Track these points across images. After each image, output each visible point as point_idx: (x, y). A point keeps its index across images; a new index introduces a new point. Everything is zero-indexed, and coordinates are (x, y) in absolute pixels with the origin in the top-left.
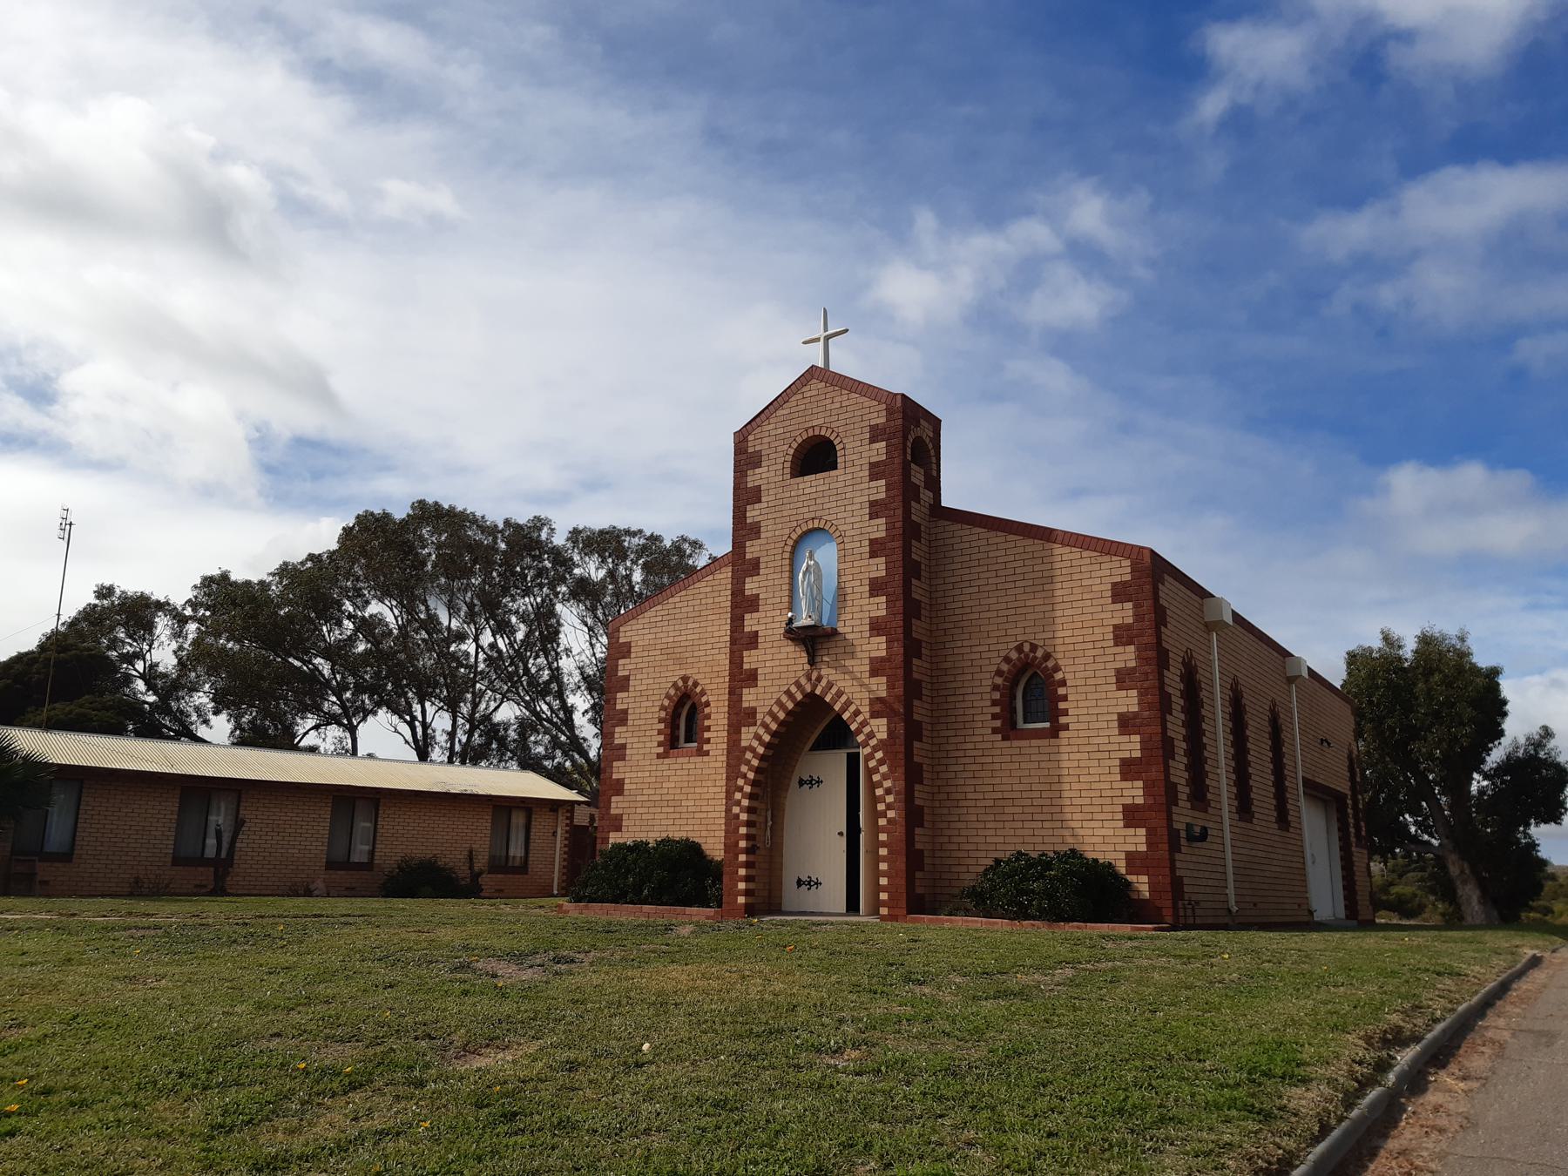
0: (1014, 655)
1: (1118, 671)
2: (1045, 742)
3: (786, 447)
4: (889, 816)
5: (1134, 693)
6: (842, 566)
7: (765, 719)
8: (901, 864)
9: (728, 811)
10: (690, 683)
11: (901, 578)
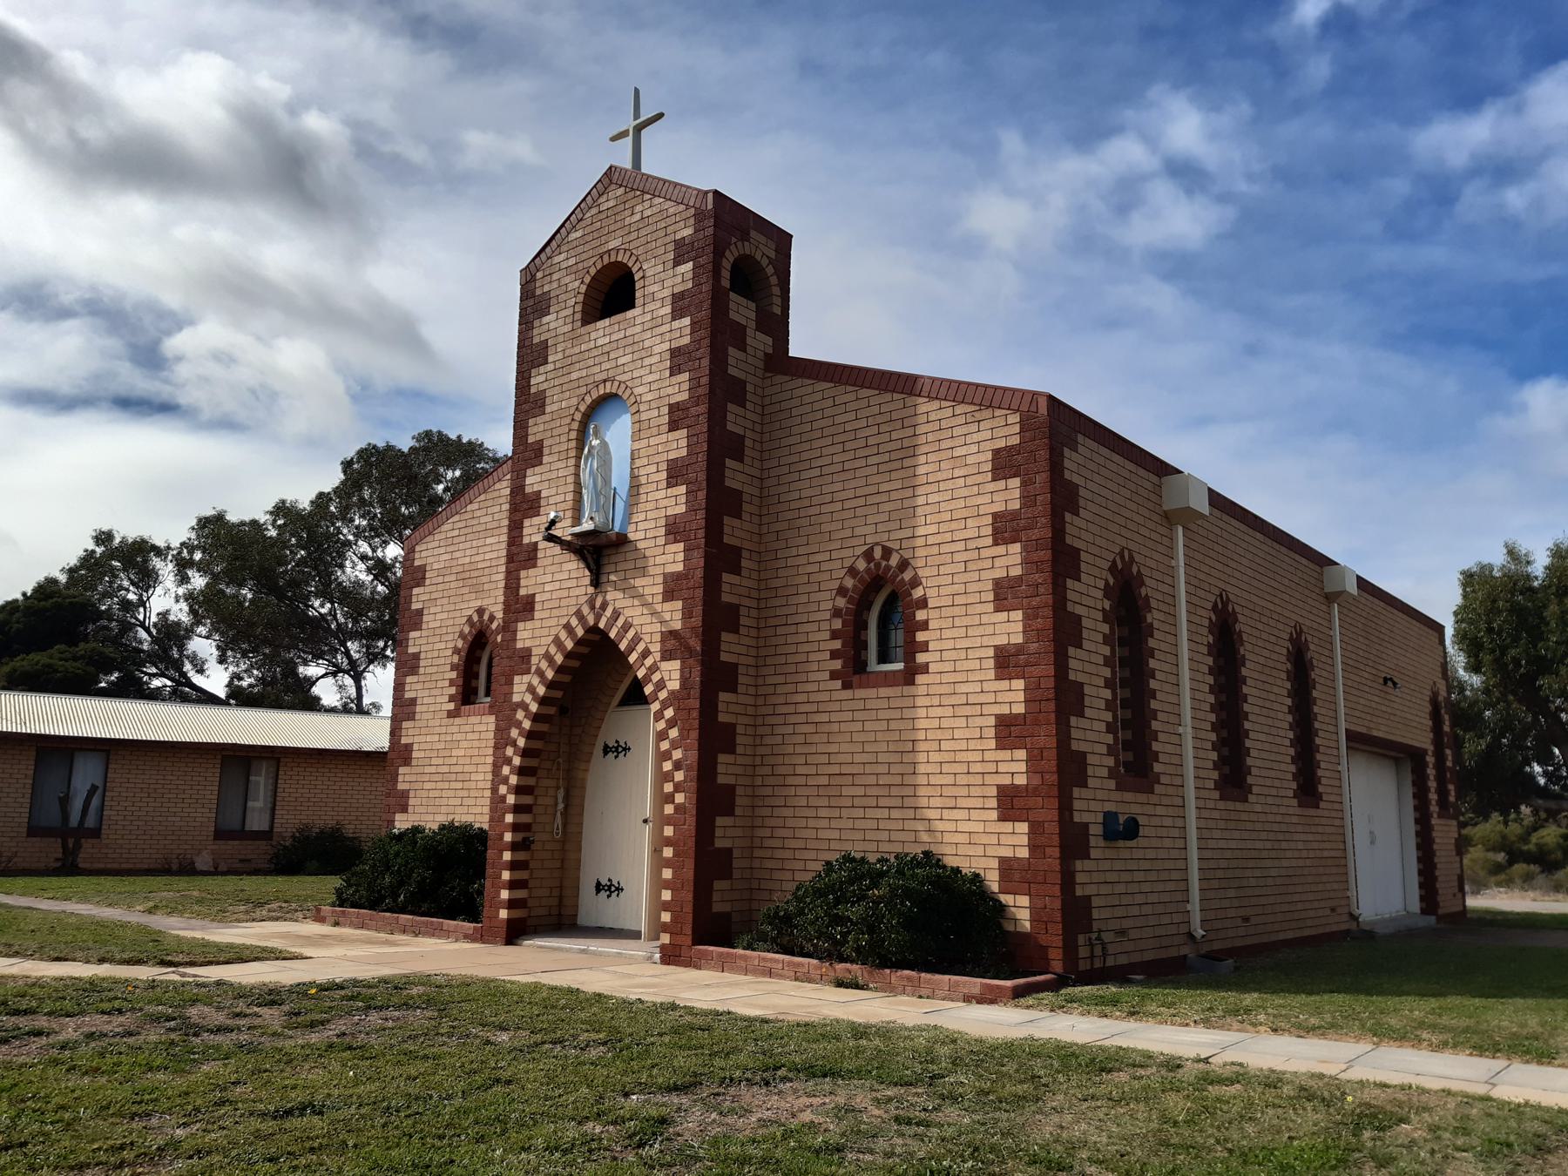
0: (861, 565)
1: (997, 583)
2: (896, 691)
3: (577, 283)
4: (676, 801)
5: (1018, 615)
6: (637, 445)
7: (540, 665)
8: (689, 872)
9: (494, 790)
10: (486, 617)
11: (705, 458)
